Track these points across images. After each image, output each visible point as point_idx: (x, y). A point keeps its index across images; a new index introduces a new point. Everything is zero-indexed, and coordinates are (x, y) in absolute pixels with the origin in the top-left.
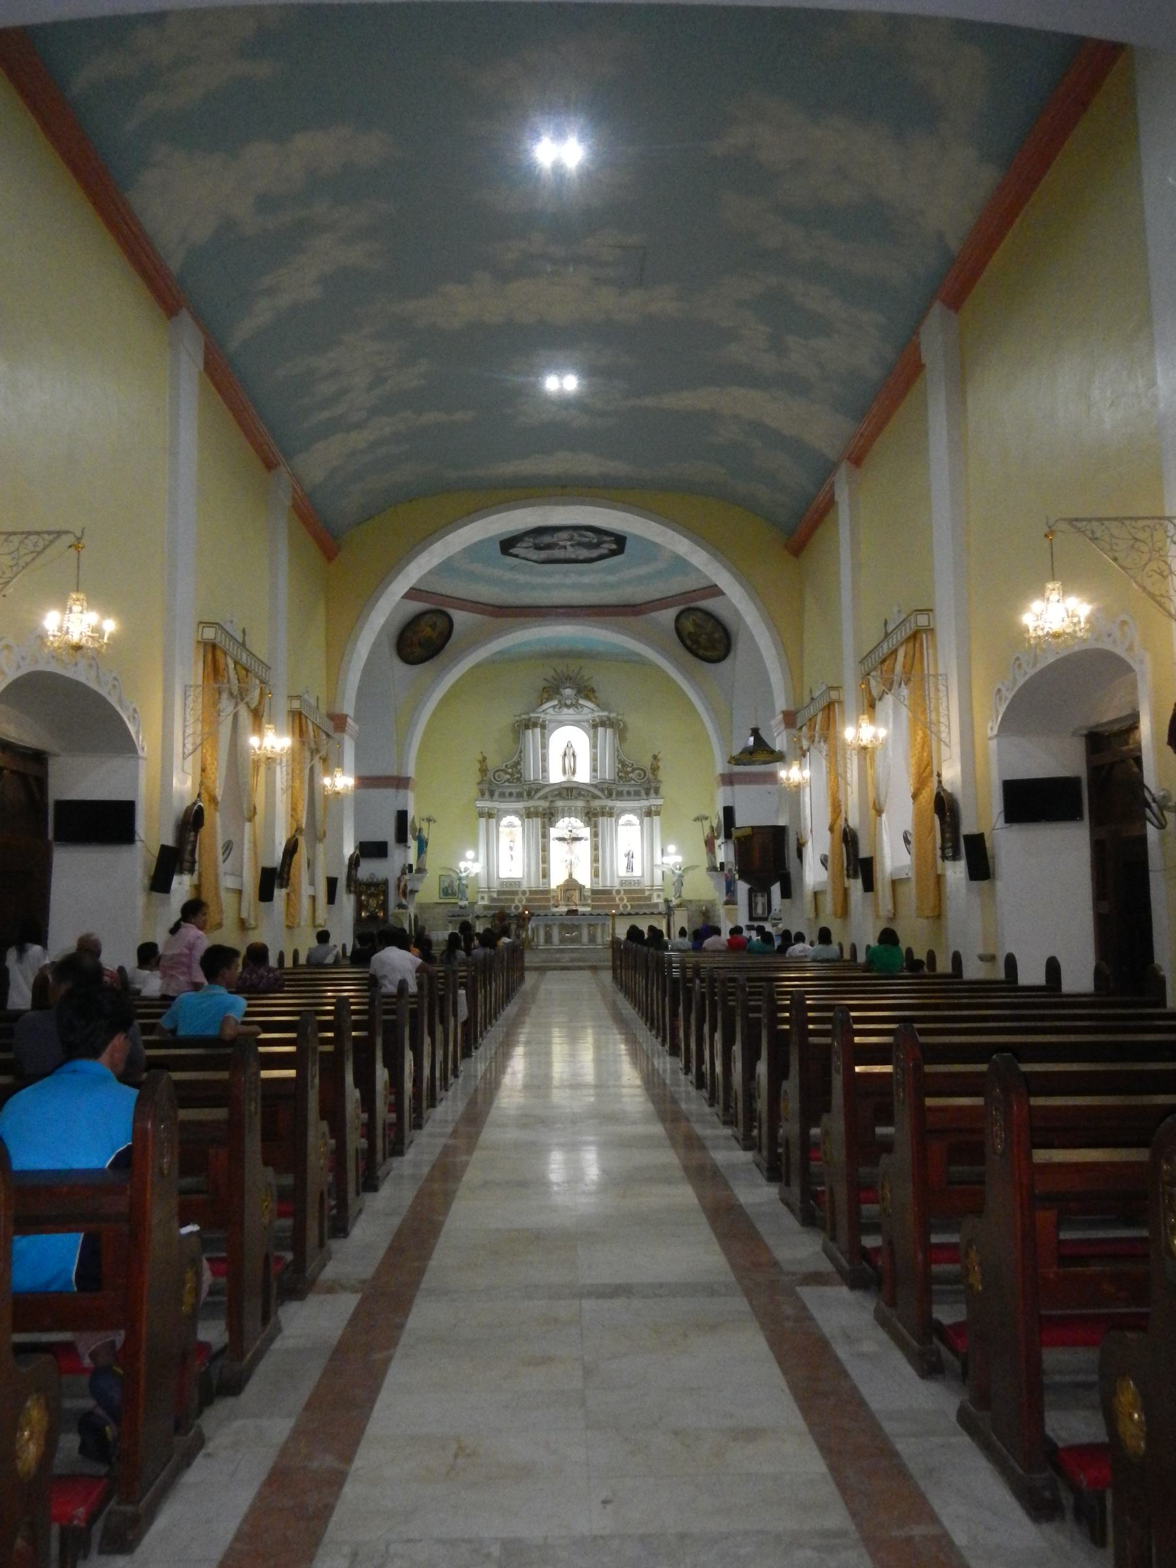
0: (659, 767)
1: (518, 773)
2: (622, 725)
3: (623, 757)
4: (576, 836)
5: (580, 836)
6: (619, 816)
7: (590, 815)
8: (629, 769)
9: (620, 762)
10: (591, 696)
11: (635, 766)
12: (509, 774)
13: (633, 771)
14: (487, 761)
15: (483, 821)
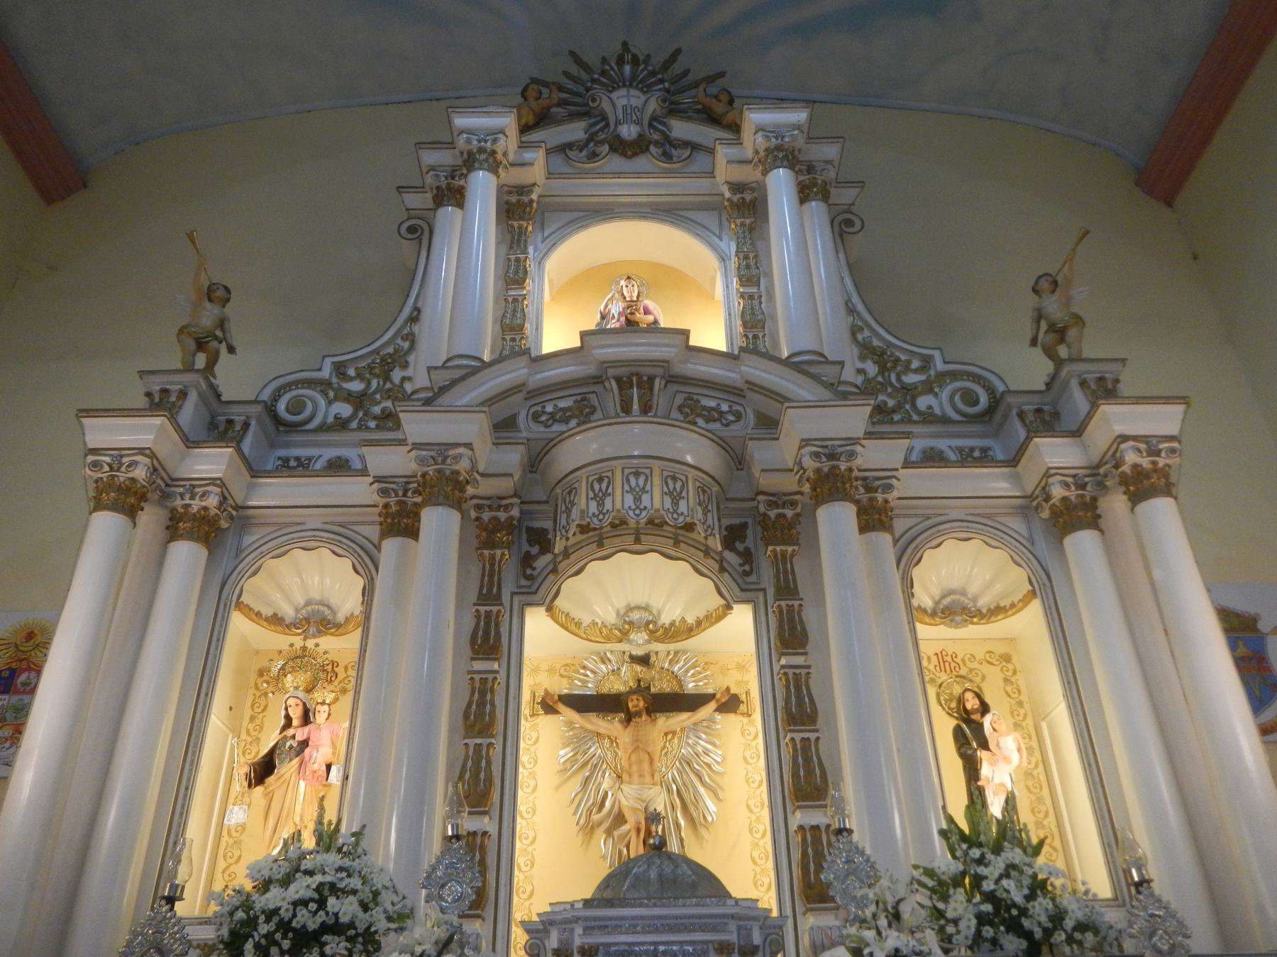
0: (1078, 320)
1: (389, 395)
2: (858, 224)
3: (881, 337)
4: (662, 686)
5: (690, 687)
6: (908, 554)
7: (752, 539)
8: (910, 379)
9: (867, 351)
10: (719, 108)
11: (940, 366)
12: (349, 397)
13: (928, 388)
14: (229, 310)
15: (105, 525)
